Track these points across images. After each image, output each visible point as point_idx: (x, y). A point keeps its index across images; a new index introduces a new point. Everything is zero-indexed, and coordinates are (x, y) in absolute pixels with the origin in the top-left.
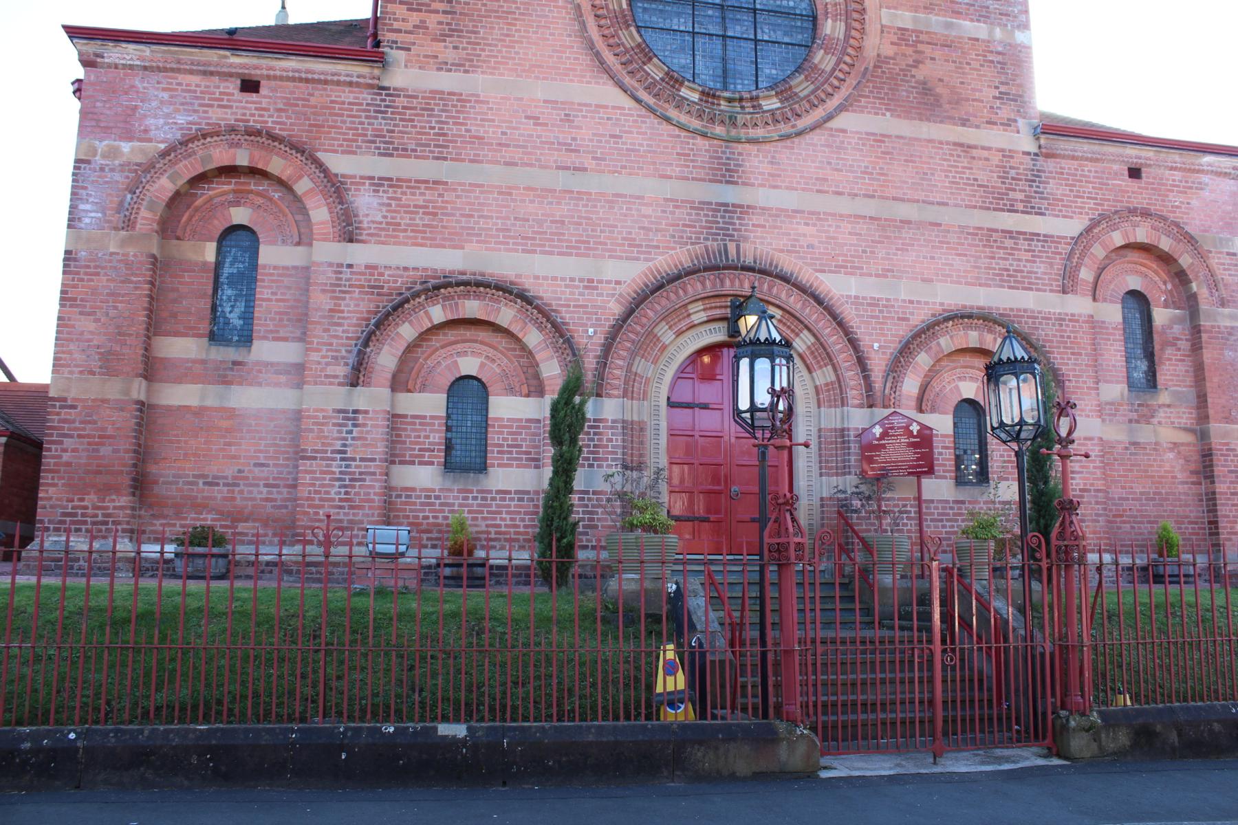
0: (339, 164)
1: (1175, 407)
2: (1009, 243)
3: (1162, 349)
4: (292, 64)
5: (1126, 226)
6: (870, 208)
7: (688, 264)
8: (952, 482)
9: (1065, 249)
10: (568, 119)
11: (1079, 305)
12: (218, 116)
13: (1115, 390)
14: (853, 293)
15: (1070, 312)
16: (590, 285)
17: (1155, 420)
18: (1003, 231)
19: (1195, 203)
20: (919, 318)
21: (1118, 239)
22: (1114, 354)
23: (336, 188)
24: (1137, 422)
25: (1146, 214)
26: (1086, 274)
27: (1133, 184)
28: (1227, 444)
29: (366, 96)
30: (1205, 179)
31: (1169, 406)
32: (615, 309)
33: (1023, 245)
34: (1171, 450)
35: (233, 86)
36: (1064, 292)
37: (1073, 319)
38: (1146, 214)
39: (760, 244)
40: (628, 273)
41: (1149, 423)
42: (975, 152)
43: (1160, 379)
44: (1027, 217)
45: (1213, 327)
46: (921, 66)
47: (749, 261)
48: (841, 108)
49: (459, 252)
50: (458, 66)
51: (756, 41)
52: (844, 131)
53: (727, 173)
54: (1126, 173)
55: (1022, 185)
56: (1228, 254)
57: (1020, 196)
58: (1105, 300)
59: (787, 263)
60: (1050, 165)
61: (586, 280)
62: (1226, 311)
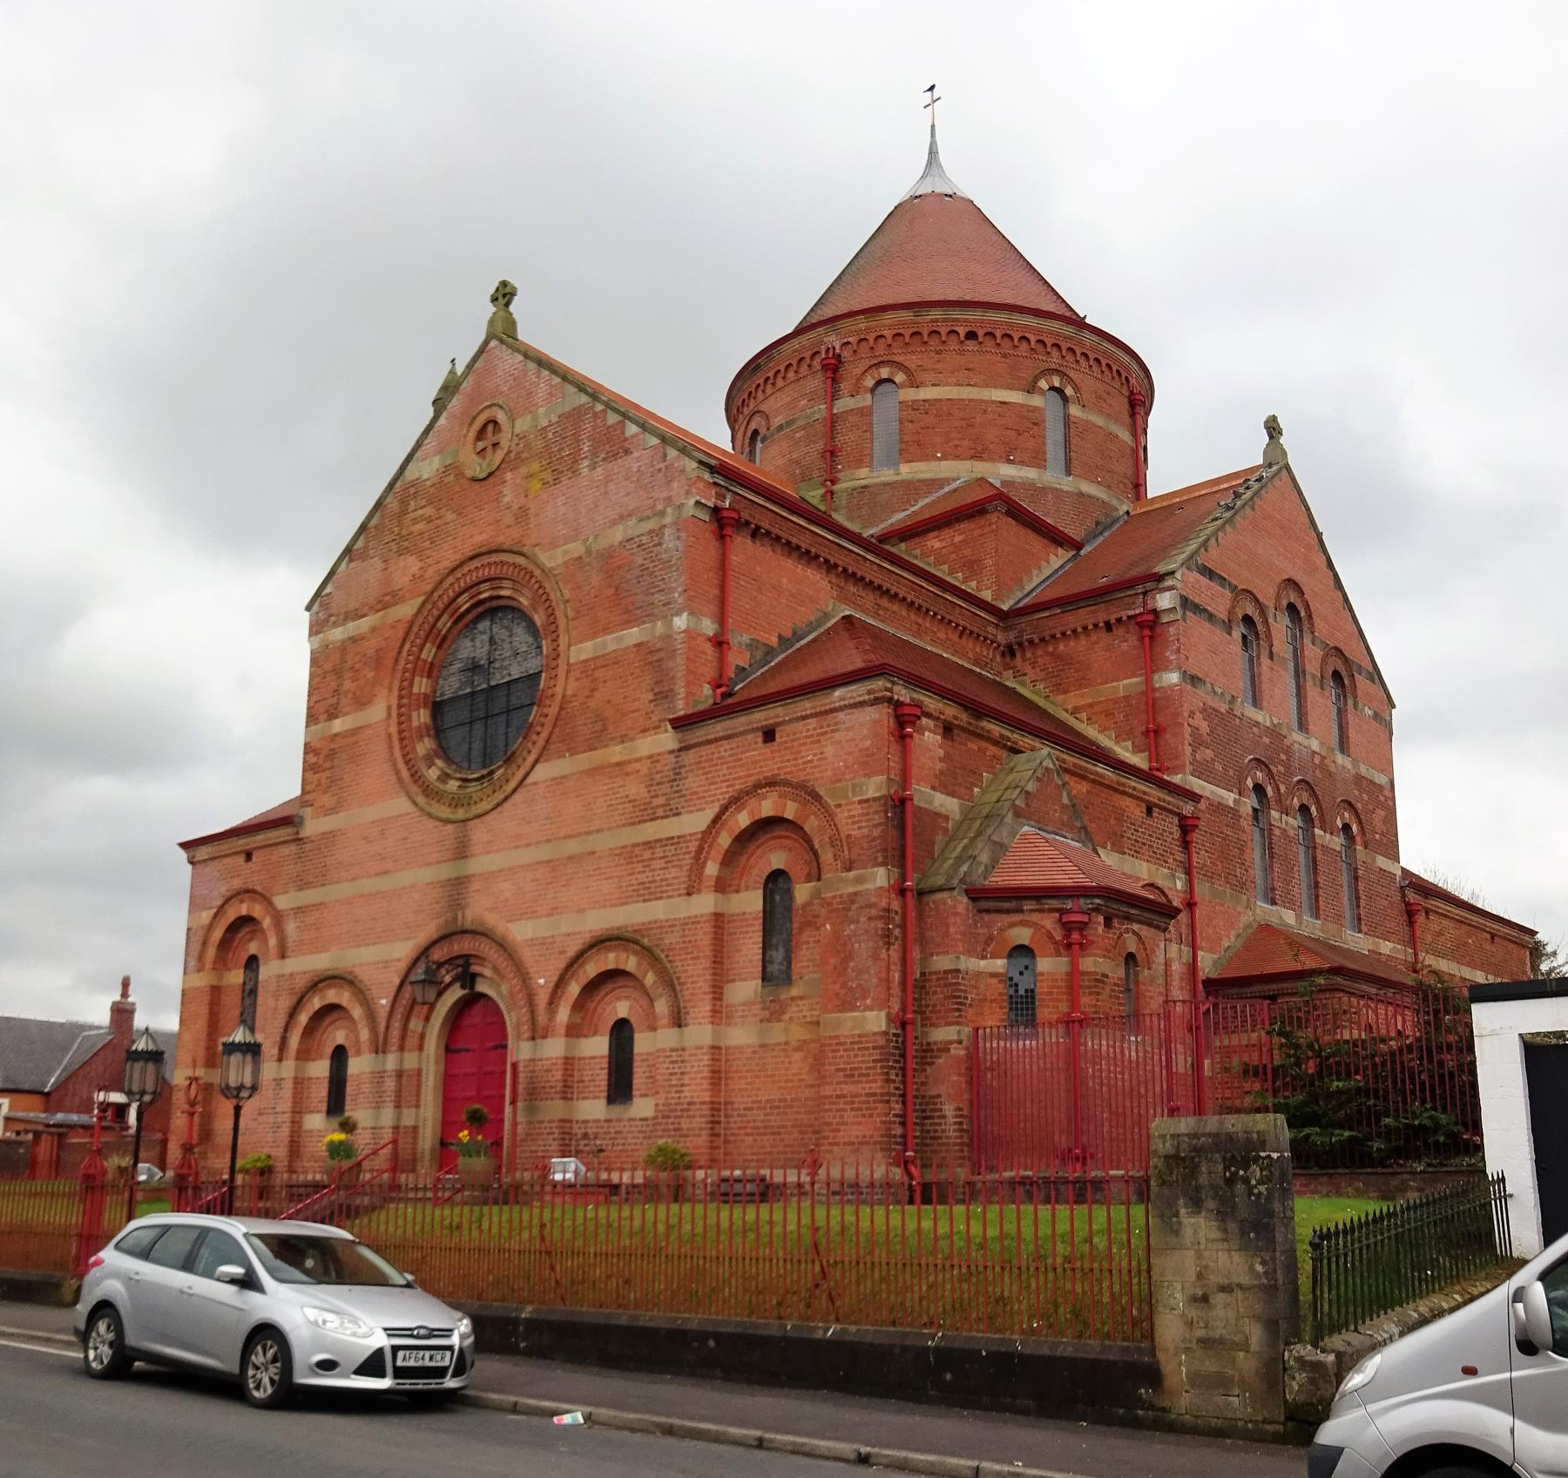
0: (281, 902)
1: (810, 997)
2: (647, 854)
3: (801, 930)
4: (260, 838)
5: (752, 803)
6: (545, 852)
7: (435, 936)
8: (602, 1102)
9: (693, 846)
10: (382, 833)
11: (705, 903)
12: (237, 883)
13: (745, 990)
14: (529, 936)
15: (693, 913)
16: (386, 964)
17: (786, 1017)
18: (645, 843)
19: (829, 750)
20: (572, 951)
21: (743, 820)
22: (749, 948)
23: (278, 918)
24: (769, 1021)
25: (772, 783)
26: (712, 869)
27: (767, 750)
28: (837, 1037)
29: (293, 848)
30: (841, 716)
31: (801, 998)
32: (397, 981)
33: (659, 852)
34: (797, 1049)
35: (241, 859)
36: (689, 894)
37: (695, 921)
38: (772, 783)
39: (479, 909)
40: (403, 950)
41: (779, 1020)
42: (629, 768)
43: (796, 967)
44: (665, 821)
45: (834, 897)
46: (596, 694)
47: (468, 925)
48: (536, 762)
49: (324, 955)
50: (333, 810)
51: (487, 717)
52: (535, 784)
53: (461, 851)
54: (760, 739)
55: (665, 789)
56: (860, 802)
57: (661, 801)
58: (747, 889)
59: (494, 921)
60: (690, 757)
61: (382, 960)
62: (852, 874)
